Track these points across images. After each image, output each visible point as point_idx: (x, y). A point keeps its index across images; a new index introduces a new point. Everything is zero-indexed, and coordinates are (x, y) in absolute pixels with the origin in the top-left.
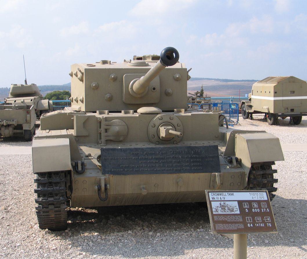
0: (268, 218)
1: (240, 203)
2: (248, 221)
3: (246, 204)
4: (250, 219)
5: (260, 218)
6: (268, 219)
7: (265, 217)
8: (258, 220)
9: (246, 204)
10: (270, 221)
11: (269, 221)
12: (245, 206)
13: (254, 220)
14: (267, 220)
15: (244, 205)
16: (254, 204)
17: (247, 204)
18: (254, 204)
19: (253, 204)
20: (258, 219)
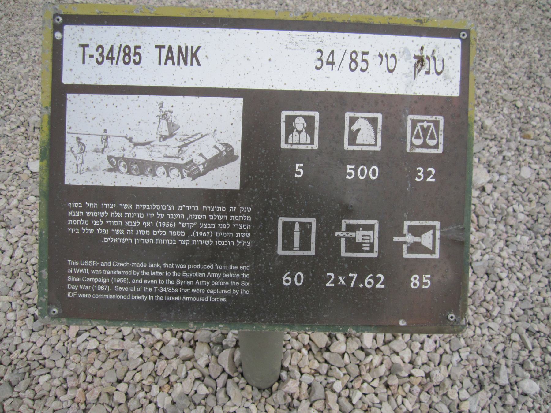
0: (426, 229)
1: (262, 110)
2: (288, 245)
3: (300, 124)
4: (305, 229)
5: (371, 228)
6: (426, 240)
7: (407, 224)
8: (359, 239)
9: (300, 124)
10: (437, 256)
11: (425, 250)
12: (294, 137)
13: (328, 242)
14: (416, 247)
15: (290, 130)
16: (363, 126)
17: (309, 120)
18: (363, 126)
19: (353, 121)
20: (359, 235)
